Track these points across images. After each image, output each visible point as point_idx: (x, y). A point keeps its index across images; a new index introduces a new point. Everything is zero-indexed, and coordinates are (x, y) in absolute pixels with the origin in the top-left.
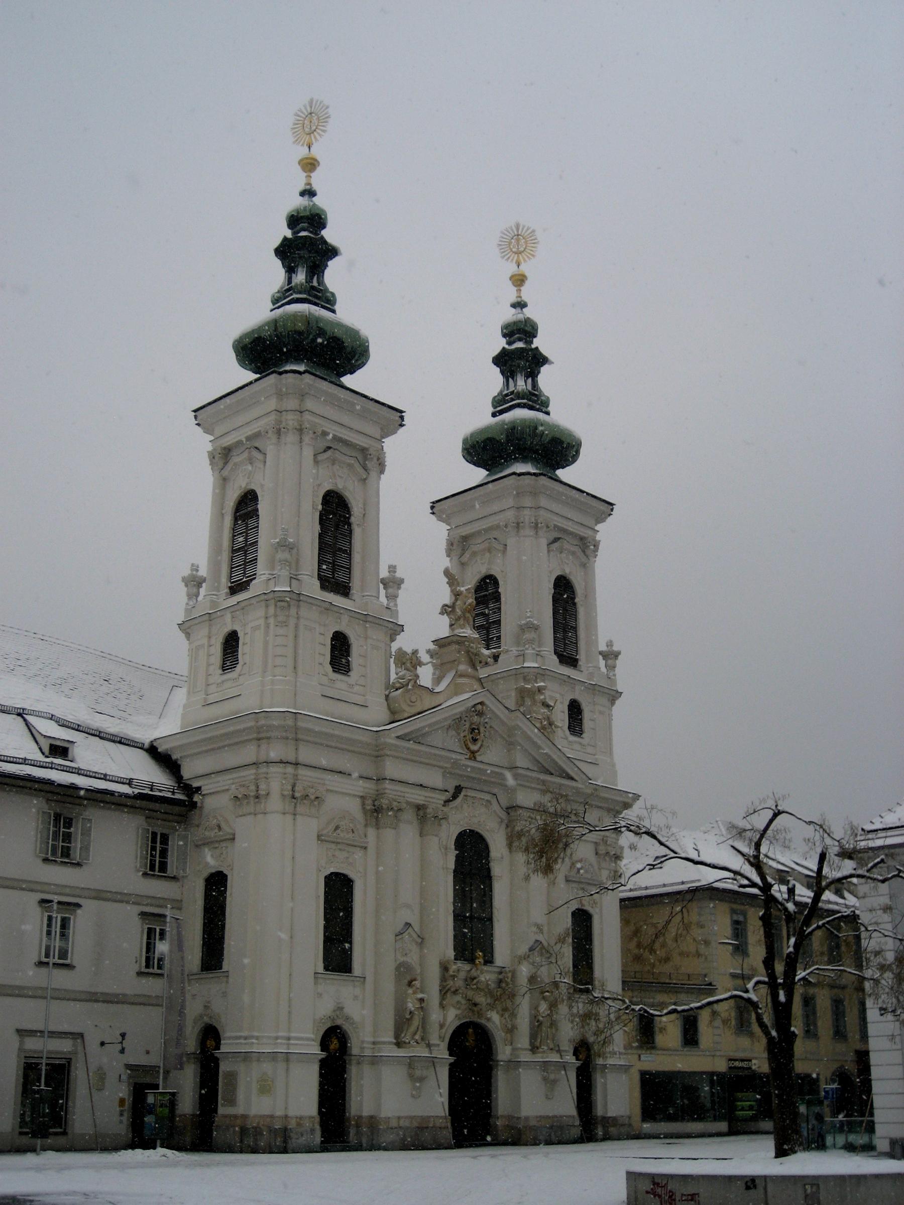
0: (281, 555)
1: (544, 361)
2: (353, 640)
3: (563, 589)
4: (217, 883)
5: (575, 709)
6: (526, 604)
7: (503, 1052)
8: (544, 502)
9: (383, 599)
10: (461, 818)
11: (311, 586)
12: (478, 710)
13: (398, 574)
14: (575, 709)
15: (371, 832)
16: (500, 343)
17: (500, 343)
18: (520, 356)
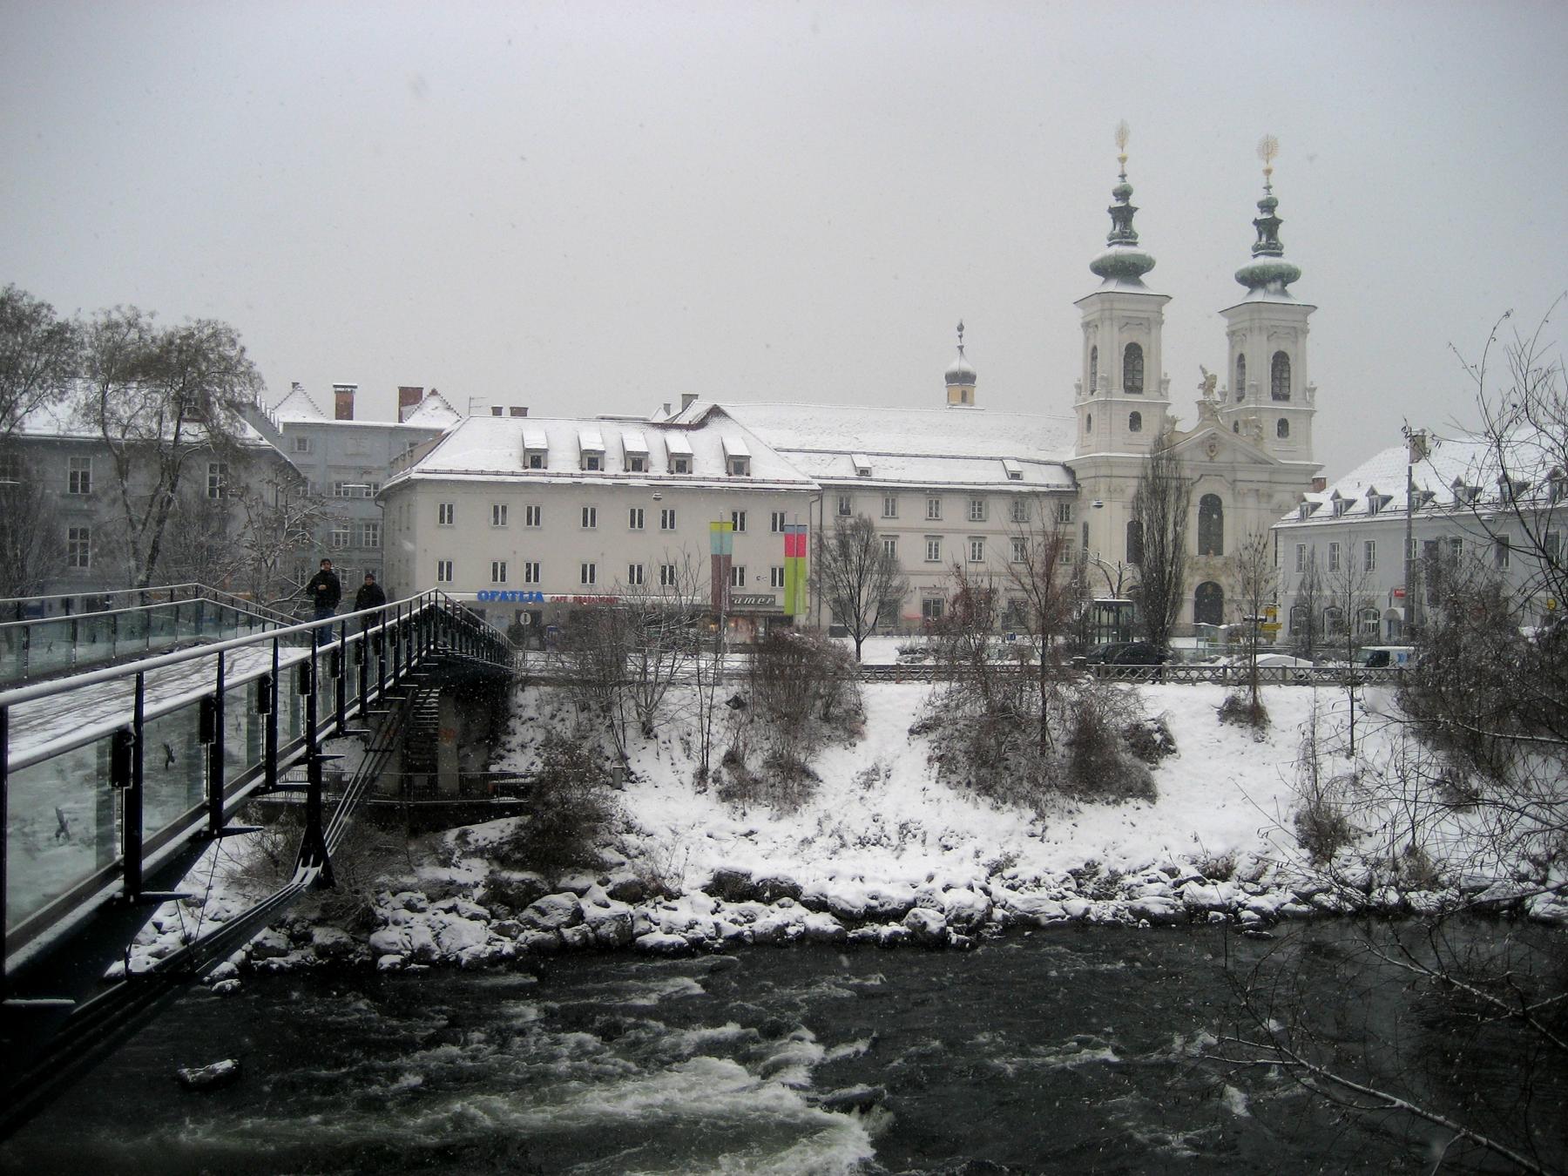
4: (1086, 527)
7: (1227, 595)
8: (1265, 315)
12: (1213, 437)
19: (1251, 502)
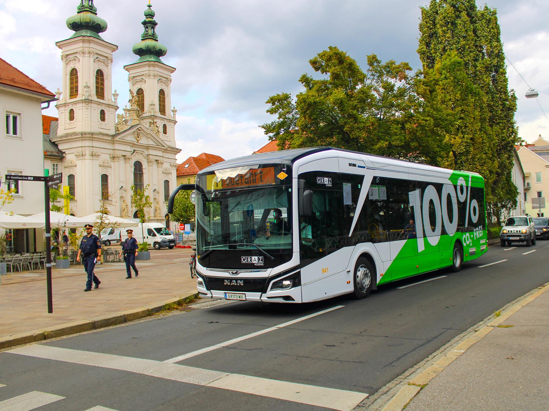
0: (86, 90)
1: (156, 24)
2: (105, 112)
3: (162, 93)
5: (165, 126)
6: (151, 99)
9: (113, 100)
10: (135, 158)
11: (95, 98)
13: (117, 93)
14: (165, 126)
15: (112, 163)
16: (144, 18)
17: (144, 18)
18: (150, 23)
19: (155, 165)
